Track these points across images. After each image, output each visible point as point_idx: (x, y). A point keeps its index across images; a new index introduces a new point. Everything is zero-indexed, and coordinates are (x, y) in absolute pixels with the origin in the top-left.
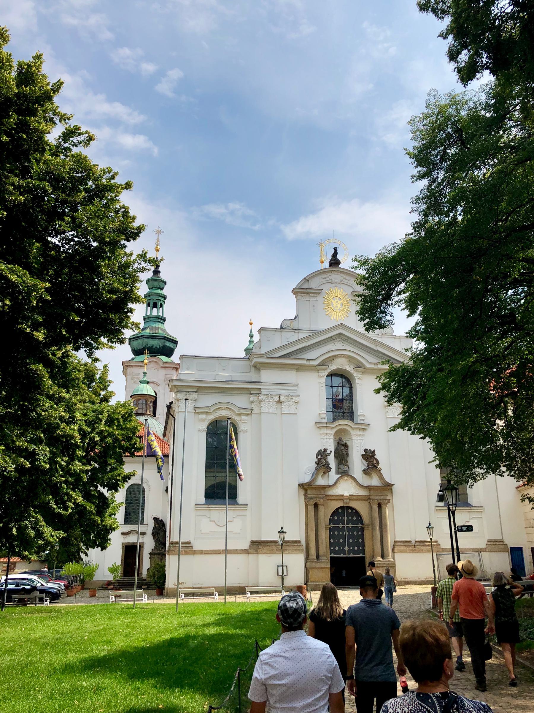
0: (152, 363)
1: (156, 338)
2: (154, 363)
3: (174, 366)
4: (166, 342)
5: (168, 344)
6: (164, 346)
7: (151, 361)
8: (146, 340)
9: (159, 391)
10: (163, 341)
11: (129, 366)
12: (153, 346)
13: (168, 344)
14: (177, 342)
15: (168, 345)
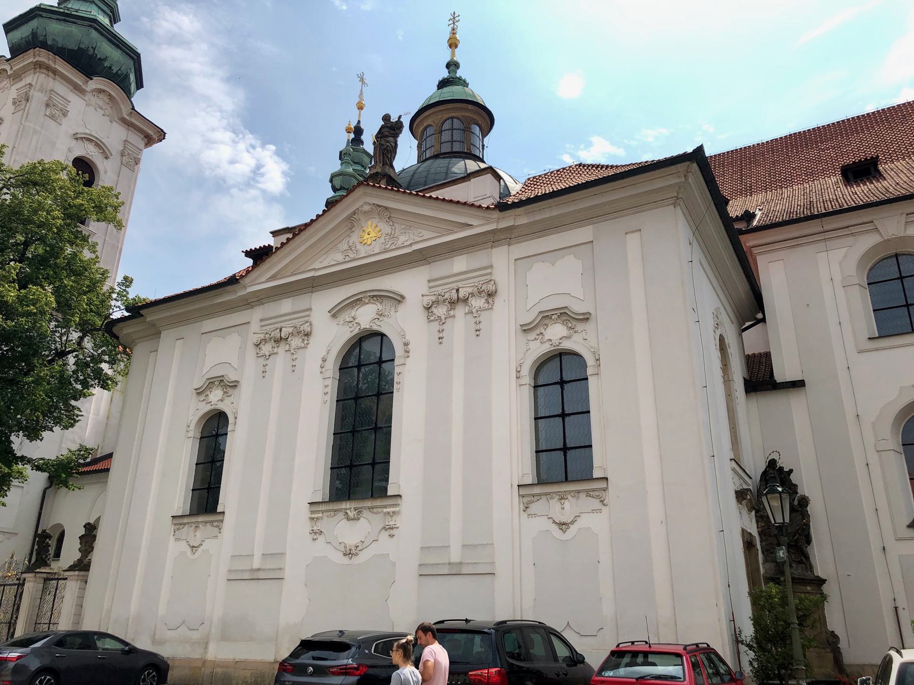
0: (101, 96)
1: (118, 47)
2: (106, 99)
3: (151, 133)
4: (133, 70)
5: (132, 77)
6: (127, 76)
7: (101, 91)
8: (94, 34)
9: (106, 172)
10: (131, 63)
11: (48, 68)
12: (106, 59)
13: (132, 77)
14: (142, 86)
15: (132, 80)
